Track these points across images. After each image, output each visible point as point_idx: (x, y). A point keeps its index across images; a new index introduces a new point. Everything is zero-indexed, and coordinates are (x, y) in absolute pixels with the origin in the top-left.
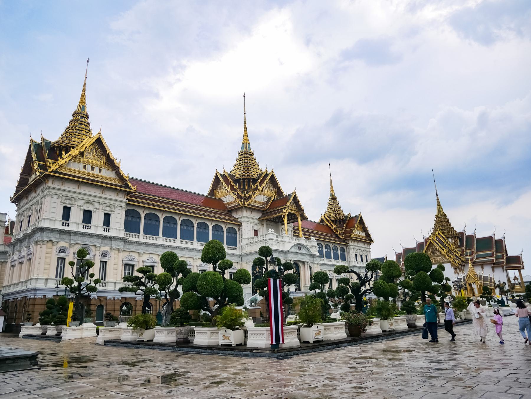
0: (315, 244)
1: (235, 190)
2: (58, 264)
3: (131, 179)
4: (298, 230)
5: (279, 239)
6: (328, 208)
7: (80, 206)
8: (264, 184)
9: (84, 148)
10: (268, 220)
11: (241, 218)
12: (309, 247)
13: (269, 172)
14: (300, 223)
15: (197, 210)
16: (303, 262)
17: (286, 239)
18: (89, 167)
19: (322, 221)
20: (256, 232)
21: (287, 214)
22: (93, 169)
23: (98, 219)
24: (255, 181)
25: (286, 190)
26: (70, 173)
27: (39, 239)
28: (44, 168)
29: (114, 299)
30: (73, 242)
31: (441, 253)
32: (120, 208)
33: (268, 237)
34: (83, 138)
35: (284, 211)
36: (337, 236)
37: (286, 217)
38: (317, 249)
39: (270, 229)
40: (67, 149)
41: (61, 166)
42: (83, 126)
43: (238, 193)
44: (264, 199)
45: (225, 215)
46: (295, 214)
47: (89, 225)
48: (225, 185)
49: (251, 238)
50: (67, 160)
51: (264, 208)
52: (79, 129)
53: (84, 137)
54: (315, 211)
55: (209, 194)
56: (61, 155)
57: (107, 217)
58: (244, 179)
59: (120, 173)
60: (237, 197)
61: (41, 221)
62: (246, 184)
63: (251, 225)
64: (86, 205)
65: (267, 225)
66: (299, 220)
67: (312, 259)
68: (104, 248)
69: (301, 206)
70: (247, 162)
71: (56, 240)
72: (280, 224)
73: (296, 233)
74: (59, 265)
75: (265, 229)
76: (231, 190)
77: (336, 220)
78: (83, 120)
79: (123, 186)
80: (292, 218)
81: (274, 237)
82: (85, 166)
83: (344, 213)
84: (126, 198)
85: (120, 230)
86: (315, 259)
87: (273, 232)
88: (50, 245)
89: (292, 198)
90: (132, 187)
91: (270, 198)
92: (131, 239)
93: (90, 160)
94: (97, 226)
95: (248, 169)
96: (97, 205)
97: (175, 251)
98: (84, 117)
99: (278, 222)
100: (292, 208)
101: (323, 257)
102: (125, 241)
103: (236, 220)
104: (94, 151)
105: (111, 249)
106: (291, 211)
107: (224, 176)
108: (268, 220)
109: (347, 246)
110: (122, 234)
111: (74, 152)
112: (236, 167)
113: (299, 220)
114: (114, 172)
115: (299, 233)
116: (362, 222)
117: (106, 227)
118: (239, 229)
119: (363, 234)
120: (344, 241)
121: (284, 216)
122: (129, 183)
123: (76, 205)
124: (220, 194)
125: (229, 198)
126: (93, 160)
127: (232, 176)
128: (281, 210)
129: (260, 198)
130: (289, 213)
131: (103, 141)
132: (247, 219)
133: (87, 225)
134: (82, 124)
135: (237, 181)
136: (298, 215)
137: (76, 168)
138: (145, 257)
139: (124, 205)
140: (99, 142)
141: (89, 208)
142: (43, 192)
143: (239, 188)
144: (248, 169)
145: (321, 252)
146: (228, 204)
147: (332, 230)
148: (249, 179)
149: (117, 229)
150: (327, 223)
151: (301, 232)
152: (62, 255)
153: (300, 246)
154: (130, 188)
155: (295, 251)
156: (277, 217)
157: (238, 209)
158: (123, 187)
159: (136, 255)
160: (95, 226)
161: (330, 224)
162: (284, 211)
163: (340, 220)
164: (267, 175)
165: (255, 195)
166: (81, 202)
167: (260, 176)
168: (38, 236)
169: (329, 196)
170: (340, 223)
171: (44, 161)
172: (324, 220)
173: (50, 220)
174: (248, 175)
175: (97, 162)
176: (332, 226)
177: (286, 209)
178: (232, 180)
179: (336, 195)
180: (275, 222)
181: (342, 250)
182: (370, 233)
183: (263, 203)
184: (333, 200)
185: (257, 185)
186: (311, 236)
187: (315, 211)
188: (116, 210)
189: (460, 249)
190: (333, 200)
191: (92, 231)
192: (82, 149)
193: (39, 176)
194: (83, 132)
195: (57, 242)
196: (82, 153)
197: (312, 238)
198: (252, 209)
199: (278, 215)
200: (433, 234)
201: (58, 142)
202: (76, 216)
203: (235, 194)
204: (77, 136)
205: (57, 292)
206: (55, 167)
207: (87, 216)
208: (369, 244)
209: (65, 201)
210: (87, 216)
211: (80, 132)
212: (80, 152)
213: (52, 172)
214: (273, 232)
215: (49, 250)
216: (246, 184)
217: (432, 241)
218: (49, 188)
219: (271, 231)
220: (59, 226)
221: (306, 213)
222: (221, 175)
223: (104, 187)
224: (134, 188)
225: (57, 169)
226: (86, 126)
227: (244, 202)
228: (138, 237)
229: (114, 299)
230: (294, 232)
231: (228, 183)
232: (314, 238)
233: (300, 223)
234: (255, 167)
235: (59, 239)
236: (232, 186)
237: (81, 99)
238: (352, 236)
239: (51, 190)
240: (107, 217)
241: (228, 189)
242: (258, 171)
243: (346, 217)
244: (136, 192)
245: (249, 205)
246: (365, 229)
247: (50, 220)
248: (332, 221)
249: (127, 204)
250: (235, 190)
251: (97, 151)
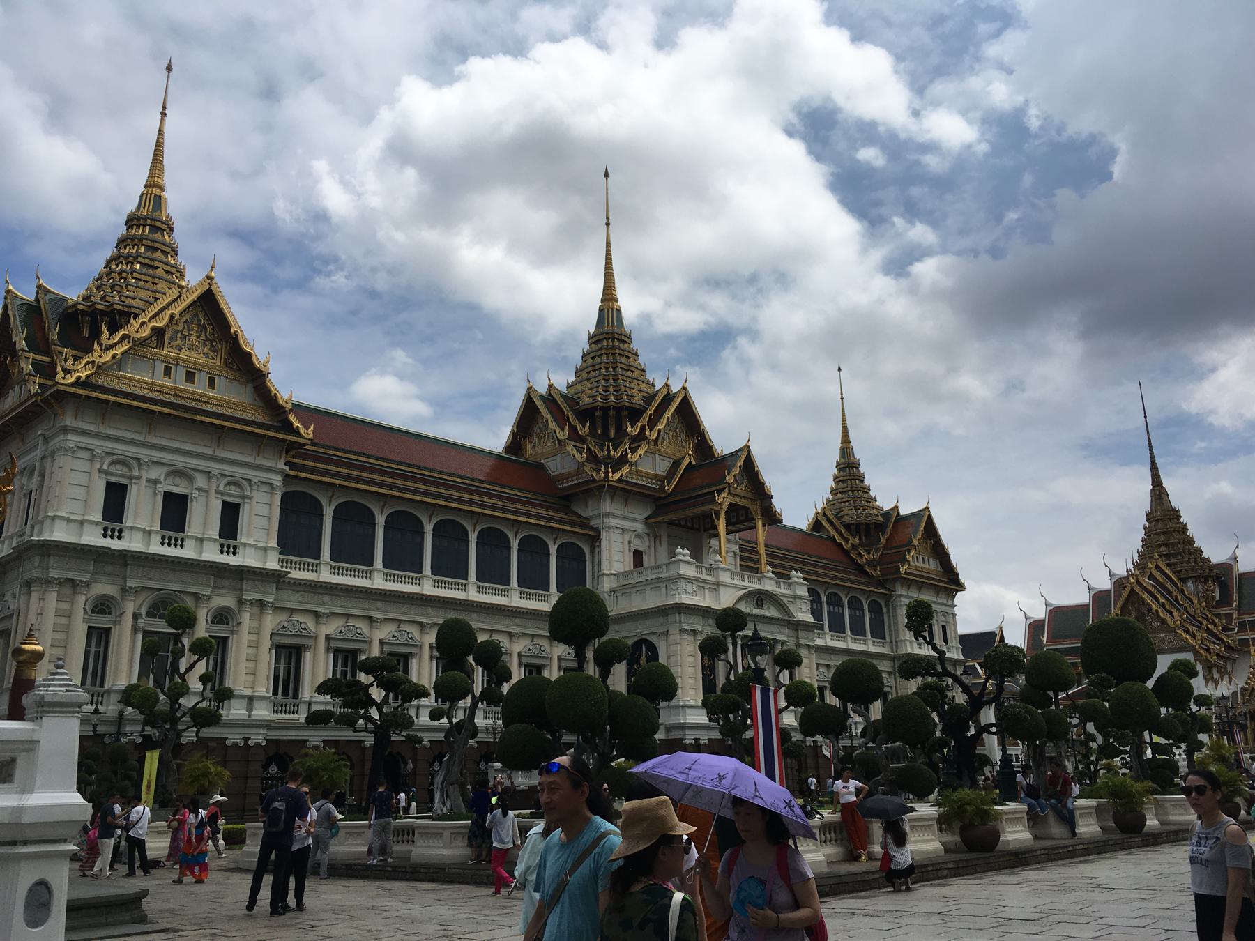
0: (803, 591)
1: (582, 439)
2: (88, 644)
3: (298, 408)
4: (757, 553)
5: (705, 576)
6: (833, 492)
7: (156, 482)
8: (661, 425)
9: (167, 319)
10: (670, 523)
11: (598, 516)
12: (785, 600)
13: (675, 388)
14: (761, 533)
17: (725, 577)
19: (817, 525)
20: (638, 556)
21: (725, 507)
22: (190, 377)
23: (203, 518)
24: (635, 414)
25: (723, 442)
26: (124, 388)
27: (36, 573)
28: (47, 371)
29: (246, 743)
30: (132, 583)
31: (1163, 621)
32: (265, 488)
33: (673, 572)
34: (158, 288)
35: (719, 499)
36: (860, 570)
37: (723, 515)
38: (806, 607)
39: (679, 550)
40: (117, 318)
41: (101, 369)
42: (158, 255)
43: (588, 449)
44: (662, 467)
45: (554, 510)
46: (746, 509)
47: (180, 535)
48: (552, 425)
49: (625, 575)
50: (119, 351)
51: (662, 487)
52: (147, 261)
53: (161, 286)
54: (799, 500)
55: (508, 449)
56: (96, 335)
58: (605, 410)
59: (269, 391)
60: (588, 460)
61: (42, 523)
62: (612, 422)
63: (627, 538)
64: (169, 481)
65: (669, 536)
66: (760, 524)
67: (792, 633)
68: (223, 600)
69: (763, 484)
70: (615, 362)
71: (84, 577)
72: (705, 535)
73: (749, 563)
74: (93, 649)
75: (663, 550)
76: (569, 438)
77: (858, 525)
78: (158, 236)
79: (273, 424)
80: (739, 519)
81: (688, 570)
82: (167, 371)
83: (879, 503)
84: (283, 461)
85: (265, 549)
86: (801, 634)
87: (688, 558)
88: (67, 591)
89: (740, 463)
90: (302, 431)
91: (676, 464)
92: (296, 574)
93: (183, 354)
95: (616, 380)
96: (201, 481)
97: (464, 616)
98: (159, 228)
99: (699, 530)
100: (738, 492)
101: (822, 628)
102: (276, 578)
103: (584, 523)
104: (195, 327)
105: (240, 602)
106: (737, 500)
107: (550, 399)
108: (670, 523)
109: (888, 598)
110: (273, 564)
111: (137, 329)
112: (584, 375)
113: (760, 524)
114: (250, 387)
115: (758, 562)
116: (930, 530)
117: (227, 542)
118: (592, 551)
119: (932, 565)
120: (881, 584)
121: (717, 514)
122: (292, 418)
123: (143, 482)
124: (540, 450)
125: (563, 459)
126: (192, 354)
127: (570, 400)
128: (709, 494)
129: (649, 464)
130: (731, 504)
131: (220, 299)
132: (613, 521)
133: (174, 534)
134: (157, 249)
135: (585, 414)
136: (756, 510)
137: (144, 378)
138: (383, 633)
139: (277, 480)
140: (208, 302)
141: (180, 488)
142: (46, 440)
143: (590, 434)
144: (616, 380)
145: (817, 614)
146: (561, 477)
147: (846, 552)
148: (618, 409)
149: (257, 547)
150: (832, 532)
151: (764, 559)
152: (101, 621)
153: (760, 598)
154: (296, 432)
156: (697, 517)
157: (591, 490)
158: (277, 429)
159: (310, 623)
160: (197, 539)
161: (841, 534)
162: (719, 499)
163: (867, 525)
164: (669, 398)
165: (638, 453)
166: (155, 473)
167: (649, 399)
168: (33, 568)
169: (836, 456)
170: (867, 534)
171: (47, 352)
172: (825, 523)
173: (68, 520)
174: (618, 397)
175: (203, 360)
176: (847, 540)
177: (725, 494)
178: (574, 412)
179: (858, 454)
180: (692, 528)
181: (876, 609)
182: (954, 560)
183: (656, 477)
184: (848, 471)
185: (643, 428)
186: (791, 569)
187: (799, 500)
188: (255, 494)
189: (1223, 611)
190: (848, 471)
192: (162, 322)
193: (37, 394)
194: (160, 272)
195: (88, 584)
196: (159, 334)
197: (794, 573)
198: (627, 493)
199: (700, 510)
200: (1140, 566)
201: (86, 298)
202: (143, 510)
203: (580, 451)
204: (141, 284)
205: (95, 726)
206: (82, 371)
207: (174, 513)
208: (951, 594)
209: (112, 469)
210: (174, 513)
211: (151, 271)
212: (153, 328)
213: (78, 383)
214: (688, 558)
215: (65, 606)
216: (612, 422)
217: (1137, 588)
218: (66, 430)
219: (683, 553)
220: (93, 538)
221: (778, 503)
222: (542, 397)
223: (218, 429)
224: (308, 433)
225: (88, 377)
226: (165, 253)
227: (606, 473)
229: (246, 743)
230: (742, 558)
231: (561, 420)
232: (799, 574)
233: (761, 533)
234: (636, 374)
235: (94, 573)
236: (573, 429)
237: (151, 175)
238: (902, 570)
239: (70, 437)
241: (563, 435)
242: (643, 387)
243: (887, 515)
244: (313, 444)
245: (619, 480)
246: (939, 552)
247: (68, 520)
248: (847, 527)
249: (287, 477)
250: (582, 439)
251: (202, 328)
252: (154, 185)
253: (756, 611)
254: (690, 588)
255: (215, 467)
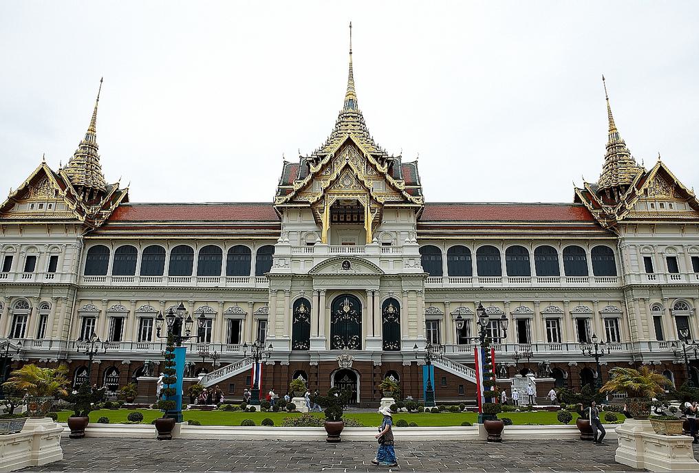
15: (255, 228)
16: (364, 292)
18: (37, 205)
23: (42, 265)
37: (327, 211)
57: (54, 260)
64: (30, 251)
94: (40, 275)
96: (42, 249)
155: (335, 272)
166: (23, 249)
191: (32, 280)
207: (30, 263)
210: (30, 263)
228: (161, 280)
240: (54, 260)
252: (92, 130)
253: (344, 272)
254: (282, 263)
255: (47, 242)
